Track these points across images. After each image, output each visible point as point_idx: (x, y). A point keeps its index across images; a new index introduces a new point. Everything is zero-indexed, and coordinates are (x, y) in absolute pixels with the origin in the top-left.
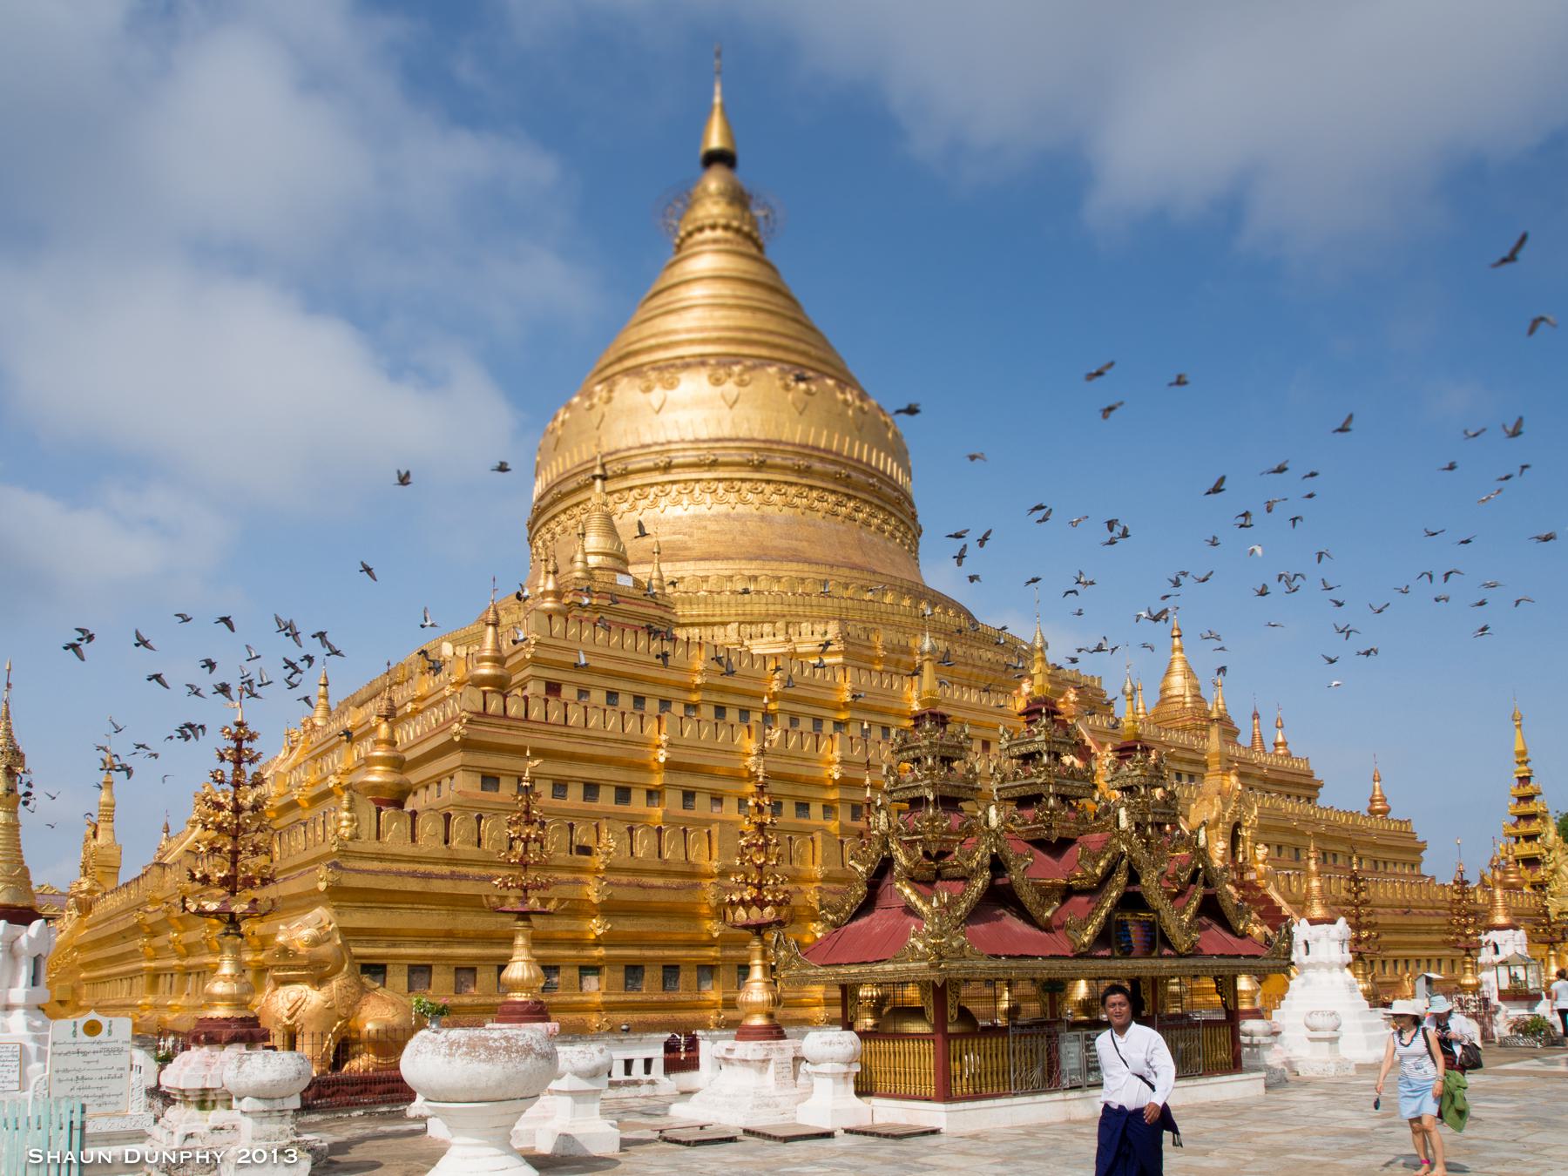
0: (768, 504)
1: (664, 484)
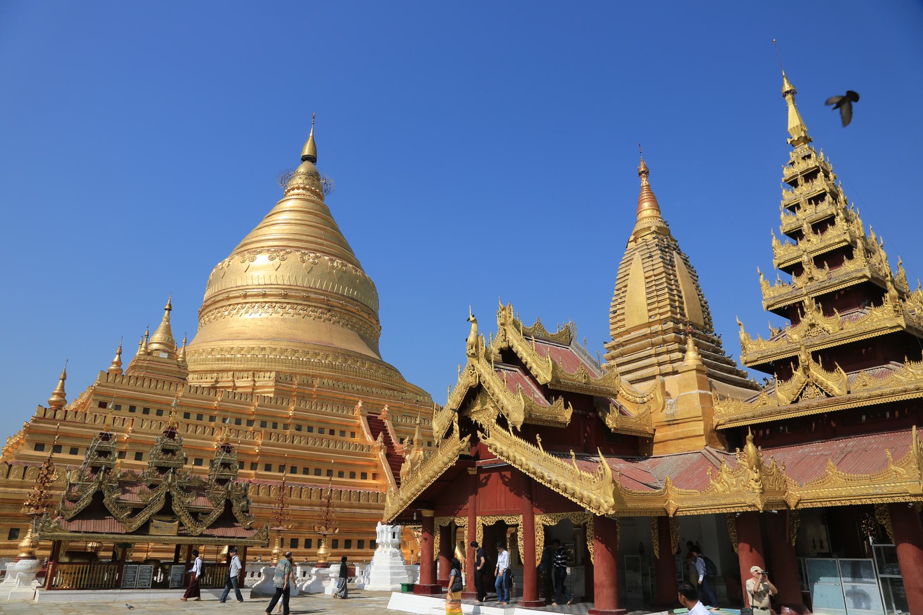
1: (242, 304)
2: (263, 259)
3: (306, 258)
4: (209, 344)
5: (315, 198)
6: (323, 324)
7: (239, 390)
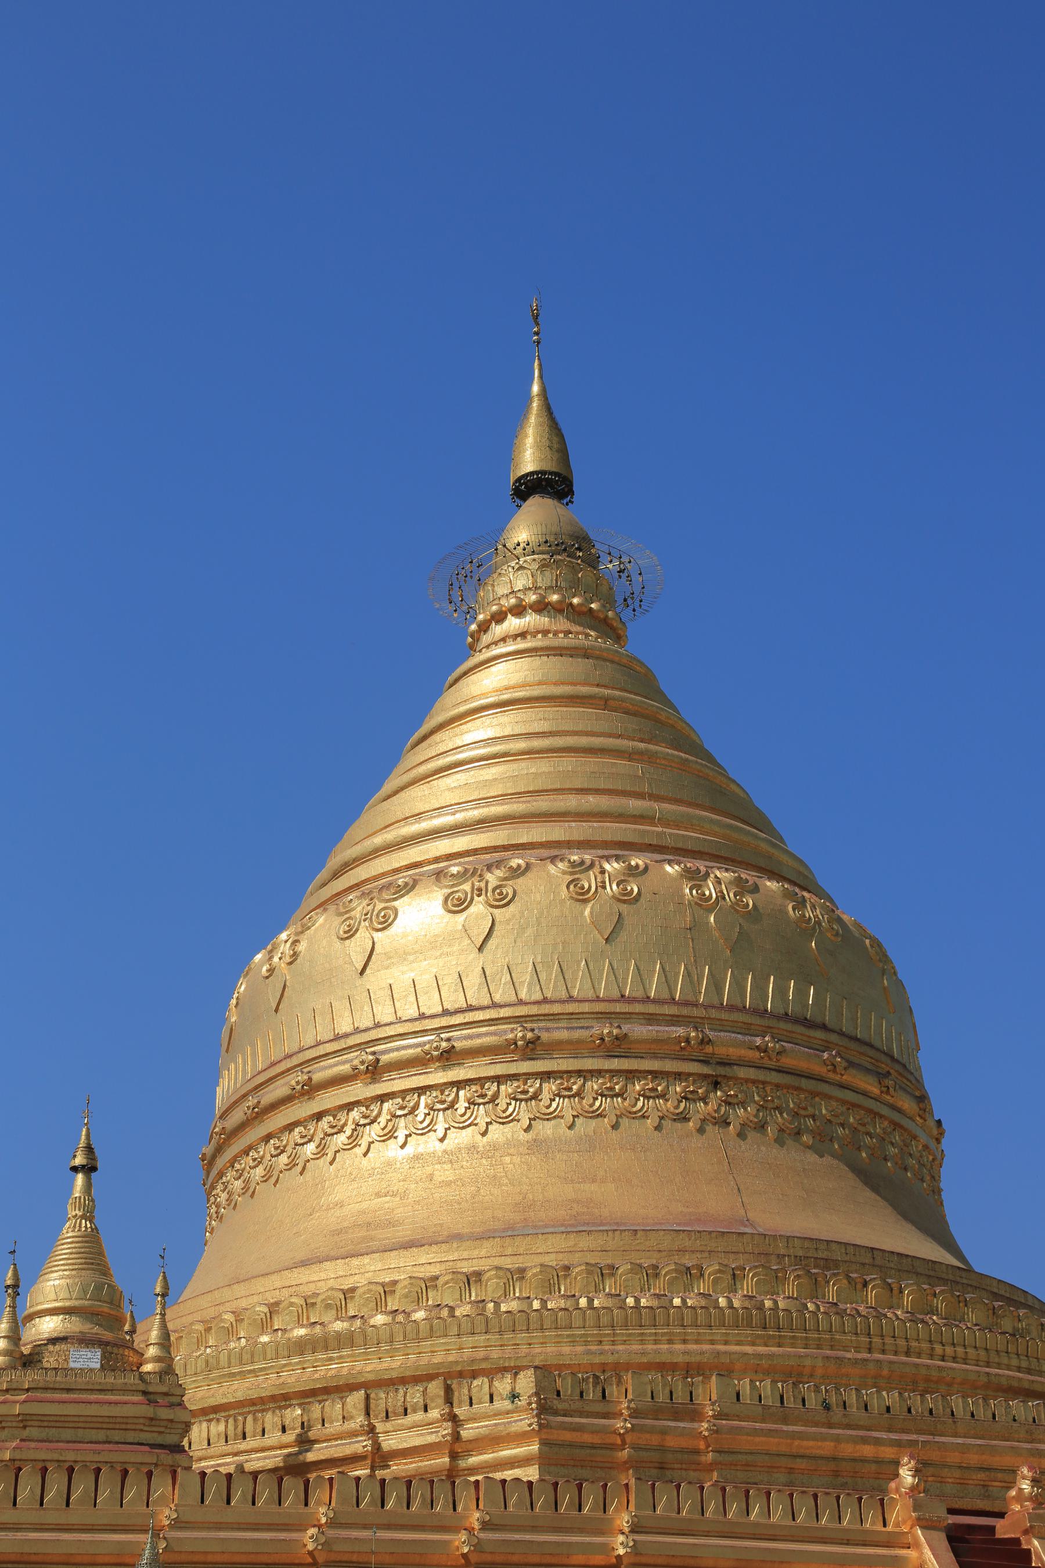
0: (548, 1117)
1: (366, 1103)
2: (421, 913)
3: (589, 881)
4: (260, 1285)
5: (592, 638)
6: (697, 1141)
7: (398, 1468)
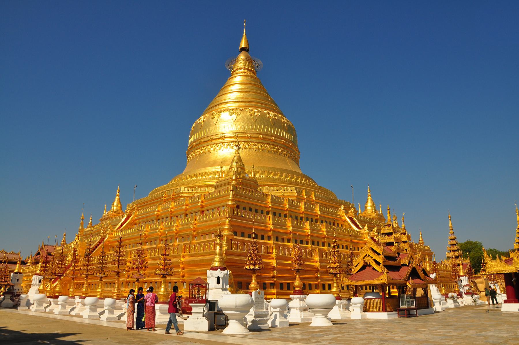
5: (252, 75)
